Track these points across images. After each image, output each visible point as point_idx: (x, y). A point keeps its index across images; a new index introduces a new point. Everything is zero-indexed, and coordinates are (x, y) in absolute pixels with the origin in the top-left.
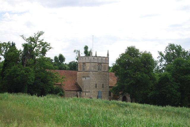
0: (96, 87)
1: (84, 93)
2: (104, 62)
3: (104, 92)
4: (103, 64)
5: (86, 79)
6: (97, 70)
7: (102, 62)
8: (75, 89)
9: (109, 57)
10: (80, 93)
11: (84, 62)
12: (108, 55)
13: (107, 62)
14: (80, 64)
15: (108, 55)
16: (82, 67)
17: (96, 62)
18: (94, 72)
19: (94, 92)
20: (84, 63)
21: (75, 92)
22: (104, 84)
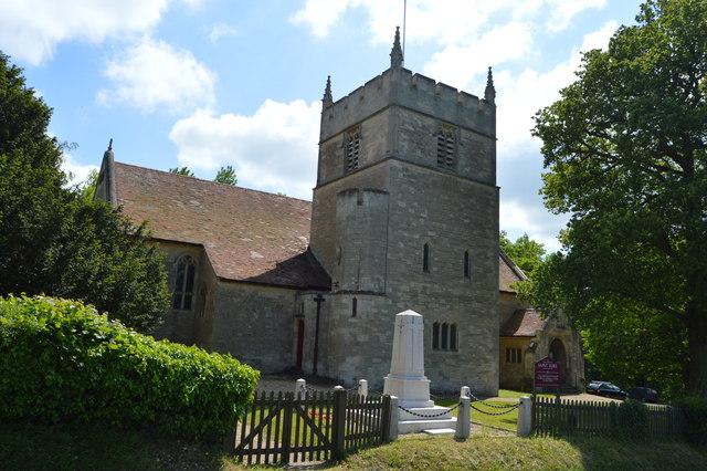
0: (426, 268)
1: (347, 300)
2: (471, 124)
3: (475, 305)
5: (360, 203)
6: (432, 160)
8: (295, 276)
9: (497, 101)
10: (319, 300)
11: (353, 121)
12: (490, 90)
13: (487, 130)
14: (331, 141)
15: (490, 90)
16: (341, 153)
17: (428, 109)
18: (415, 169)
20: (351, 129)
21: (289, 295)
22: (471, 252)
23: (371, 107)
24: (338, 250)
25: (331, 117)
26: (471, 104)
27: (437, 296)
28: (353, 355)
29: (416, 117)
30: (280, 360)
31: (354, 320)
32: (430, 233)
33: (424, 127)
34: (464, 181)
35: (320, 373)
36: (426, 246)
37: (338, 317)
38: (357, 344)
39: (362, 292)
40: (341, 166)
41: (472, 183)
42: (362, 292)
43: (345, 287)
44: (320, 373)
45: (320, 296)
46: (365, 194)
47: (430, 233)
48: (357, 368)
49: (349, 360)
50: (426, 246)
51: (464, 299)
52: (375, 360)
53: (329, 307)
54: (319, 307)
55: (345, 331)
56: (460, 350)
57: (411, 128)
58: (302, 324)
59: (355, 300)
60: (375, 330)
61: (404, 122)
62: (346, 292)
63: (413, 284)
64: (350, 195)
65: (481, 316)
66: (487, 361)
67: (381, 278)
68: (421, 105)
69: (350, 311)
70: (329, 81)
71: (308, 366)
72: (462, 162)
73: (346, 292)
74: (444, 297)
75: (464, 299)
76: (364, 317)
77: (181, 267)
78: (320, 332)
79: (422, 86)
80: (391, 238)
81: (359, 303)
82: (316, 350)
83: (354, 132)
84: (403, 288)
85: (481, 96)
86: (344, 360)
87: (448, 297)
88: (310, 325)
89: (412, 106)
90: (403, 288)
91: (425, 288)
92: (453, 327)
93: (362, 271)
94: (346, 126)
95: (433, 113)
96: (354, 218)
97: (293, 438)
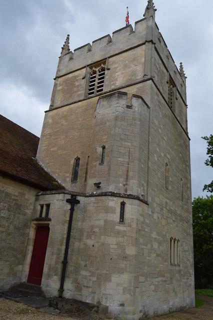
11: (97, 58)
14: (70, 76)
20: (91, 66)
23: (114, 49)
24: (100, 150)
25: (71, 59)
28: (121, 271)
30: (8, 274)
31: (121, 228)
35: (67, 295)
37: (102, 223)
38: (126, 258)
39: (130, 197)
40: (83, 92)
42: (130, 197)
43: (111, 188)
44: (67, 295)
46: (134, 100)
48: (125, 290)
49: (115, 278)
53: (85, 210)
54: (72, 210)
55: (112, 241)
58: (43, 231)
59: (123, 204)
62: (113, 195)
64: (119, 97)
70: (68, 38)
71: (50, 284)
73: (113, 195)
76: (134, 226)
78: (71, 239)
81: (128, 207)
83: (99, 68)
86: (108, 279)
87: (174, 213)
88: (57, 231)
93: (131, 174)
94: (90, 62)
96: (123, 119)
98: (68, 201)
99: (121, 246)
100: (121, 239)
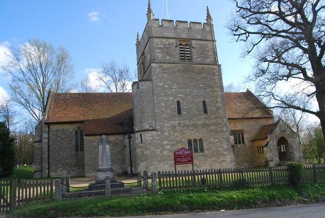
0: (179, 112)
2: (199, 37)
3: (212, 128)
4: (194, 42)
5: (138, 88)
6: (177, 58)
7: (193, 38)
9: (213, 22)
10: (130, 138)
13: (209, 37)
18: (165, 66)
19: (173, 127)
22: (207, 100)
26: (197, 26)
27: (188, 126)
28: (143, 161)
29: (164, 40)
30: (120, 168)
31: (141, 145)
32: (179, 95)
33: (169, 44)
34: (197, 65)
35: (134, 172)
36: (178, 102)
39: (144, 131)
41: (202, 66)
42: (142, 131)
43: (137, 130)
44: (134, 172)
45: (130, 136)
47: (179, 95)
50: (178, 102)
51: (204, 125)
52: (154, 163)
54: (130, 141)
56: (206, 152)
57: (162, 46)
59: (141, 135)
60: (152, 148)
61: (157, 44)
63: (172, 122)
65: (217, 132)
66: (224, 155)
67: (153, 122)
68: (166, 34)
69: (139, 141)
72: (195, 57)
74: (192, 126)
75: (204, 125)
77: (76, 133)
79: (166, 24)
80: (156, 102)
82: (131, 161)
84: (166, 125)
85: (203, 20)
86: (139, 165)
89: (161, 36)
90: (166, 125)
91: (180, 124)
92: (201, 140)
95: (174, 36)
97: (9, 189)
98: (128, 138)
99: (142, 152)
100: (141, 149)
